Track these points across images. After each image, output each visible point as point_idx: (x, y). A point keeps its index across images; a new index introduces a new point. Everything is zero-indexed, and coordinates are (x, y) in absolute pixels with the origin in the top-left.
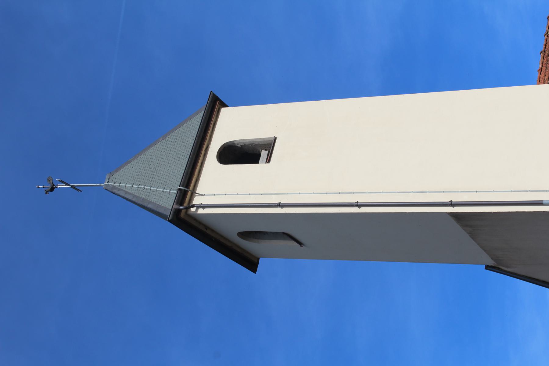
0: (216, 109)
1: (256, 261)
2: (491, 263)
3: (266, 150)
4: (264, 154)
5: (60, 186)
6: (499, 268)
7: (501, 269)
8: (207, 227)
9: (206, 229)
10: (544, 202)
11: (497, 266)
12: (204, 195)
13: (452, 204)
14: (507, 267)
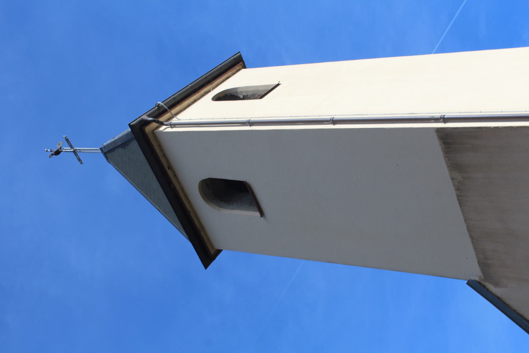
0: (237, 67)
1: (212, 252)
2: (476, 274)
5: (65, 149)
6: (485, 286)
7: (487, 289)
8: (170, 167)
9: (168, 167)
11: (483, 283)
13: (445, 120)
14: (496, 284)
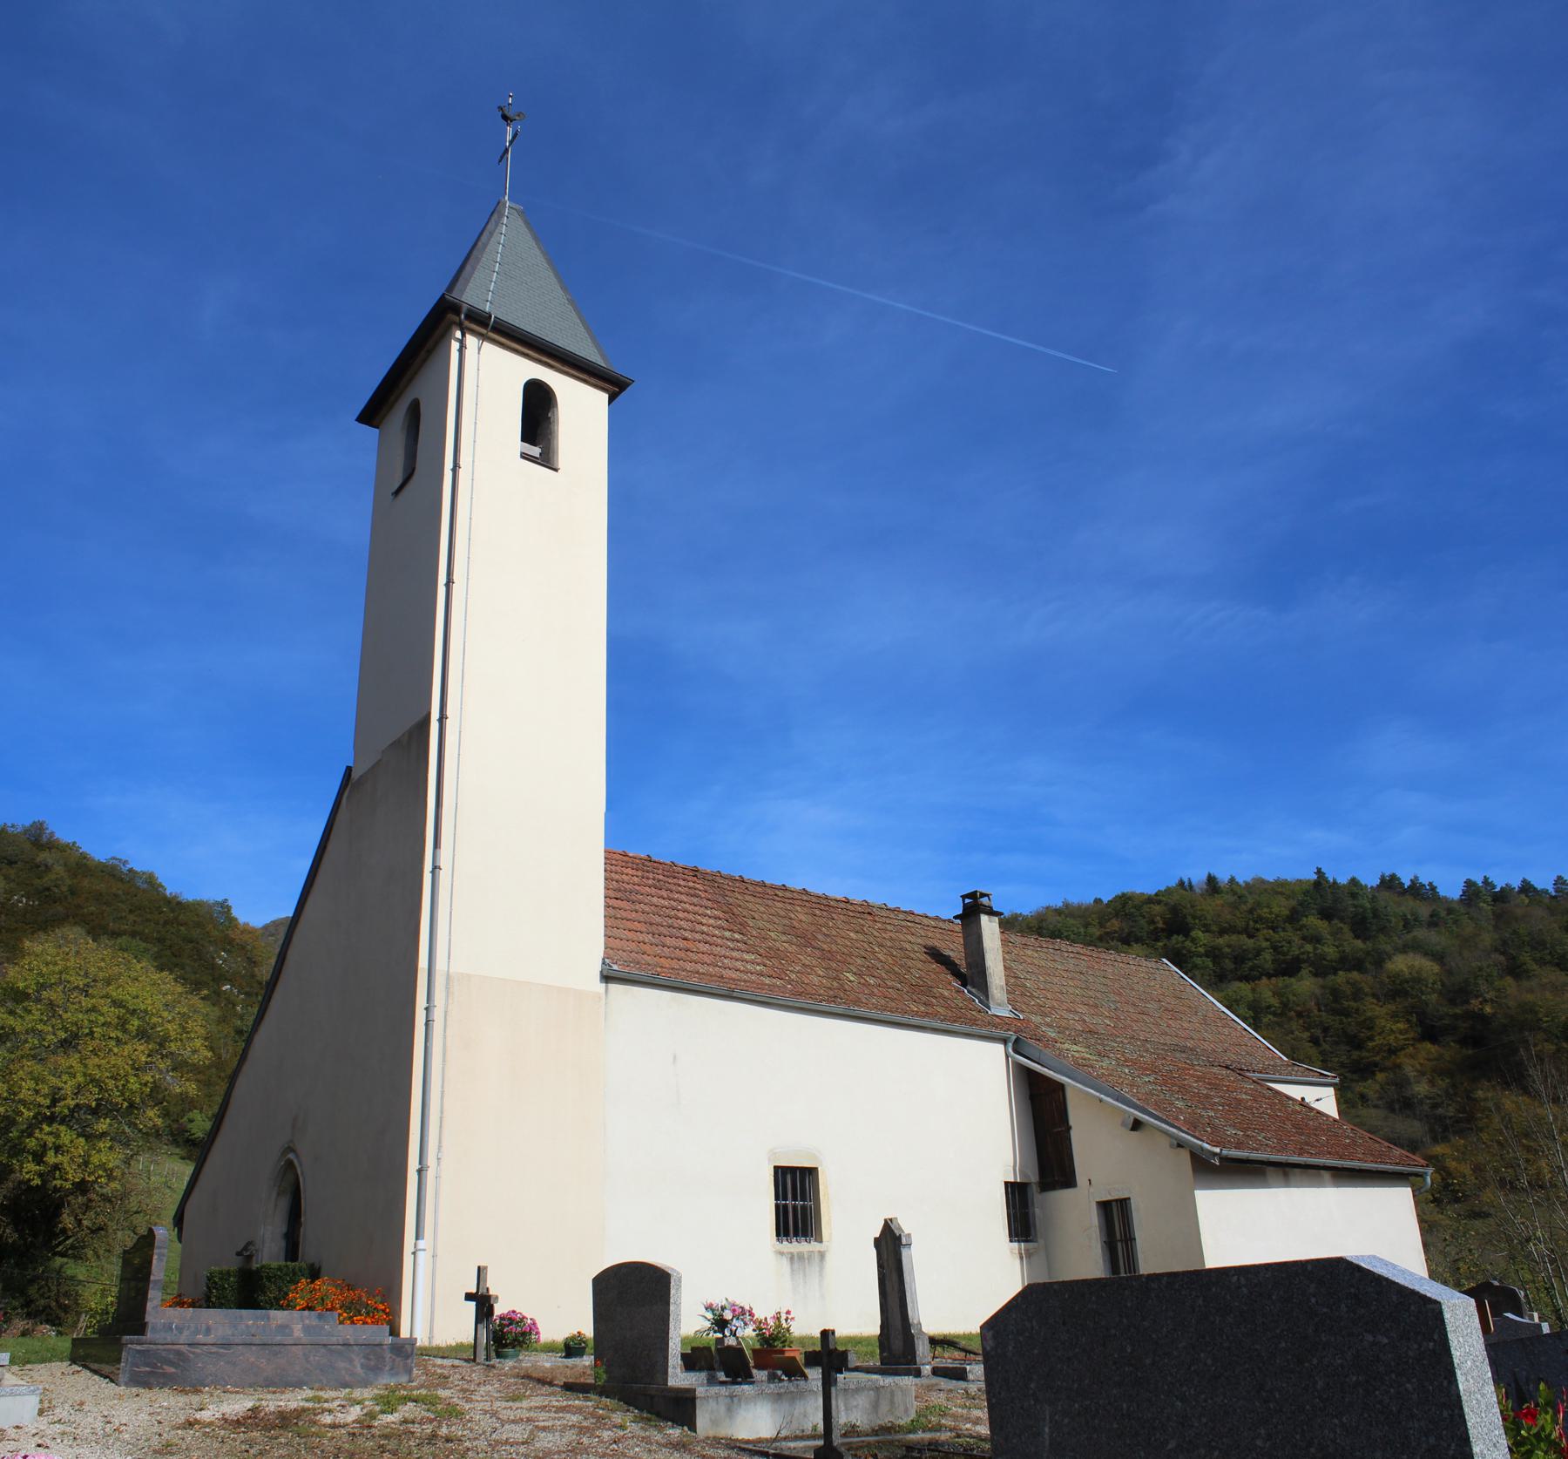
3: (541, 454)
4: (535, 451)
8: (430, 352)
10: (438, 850)
12: (479, 353)
13: (442, 718)
